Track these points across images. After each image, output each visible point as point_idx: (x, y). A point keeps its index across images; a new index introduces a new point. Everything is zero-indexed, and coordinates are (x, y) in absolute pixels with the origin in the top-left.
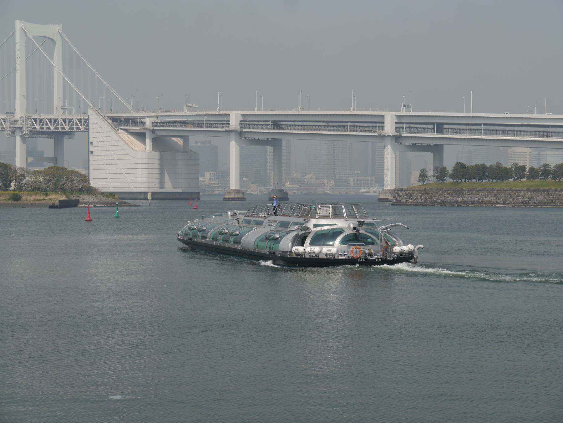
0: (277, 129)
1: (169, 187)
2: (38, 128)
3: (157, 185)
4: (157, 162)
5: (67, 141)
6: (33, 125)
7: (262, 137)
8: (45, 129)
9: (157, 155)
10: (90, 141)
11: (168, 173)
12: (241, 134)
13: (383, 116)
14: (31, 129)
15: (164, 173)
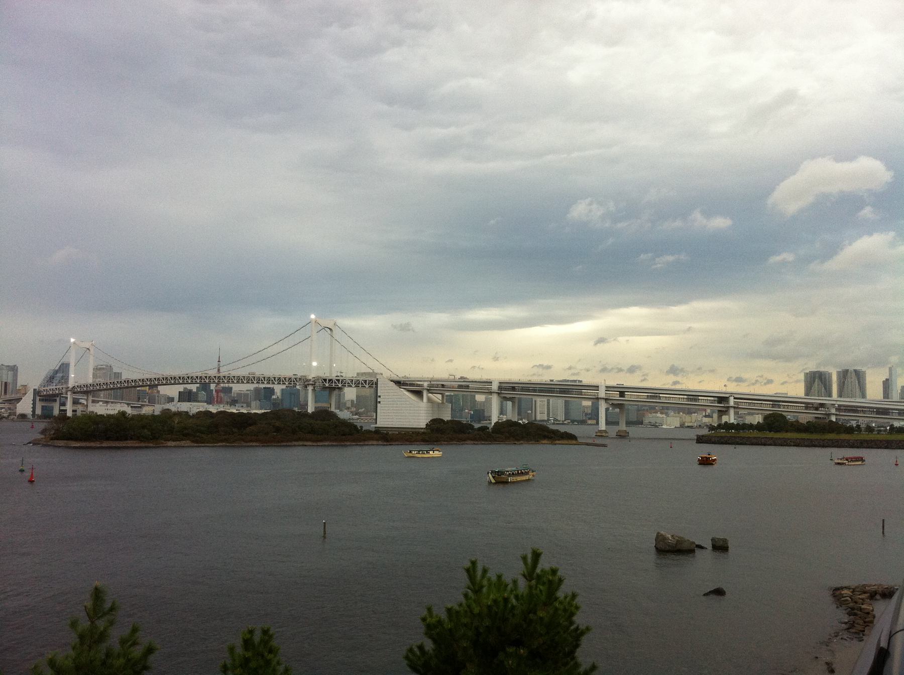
0: (514, 391)
2: (327, 385)
5: (336, 392)
6: (323, 383)
7: (508, 396)
8: (333, 386)
10: (378, 395)
12: (499, 394)
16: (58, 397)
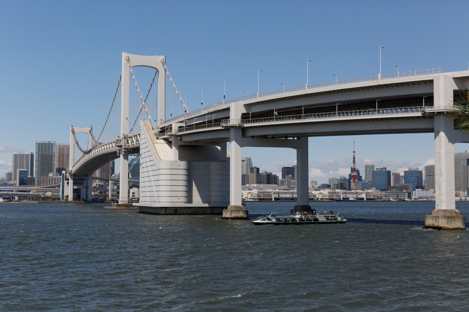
1: (197, 201)
3: (183, 199)
4: (184, 172)
9: (183, 164)
11: (196, 186)
13: (431, 82)
14: (126, 147)
15: (192, 185)
16: (85, 180)
